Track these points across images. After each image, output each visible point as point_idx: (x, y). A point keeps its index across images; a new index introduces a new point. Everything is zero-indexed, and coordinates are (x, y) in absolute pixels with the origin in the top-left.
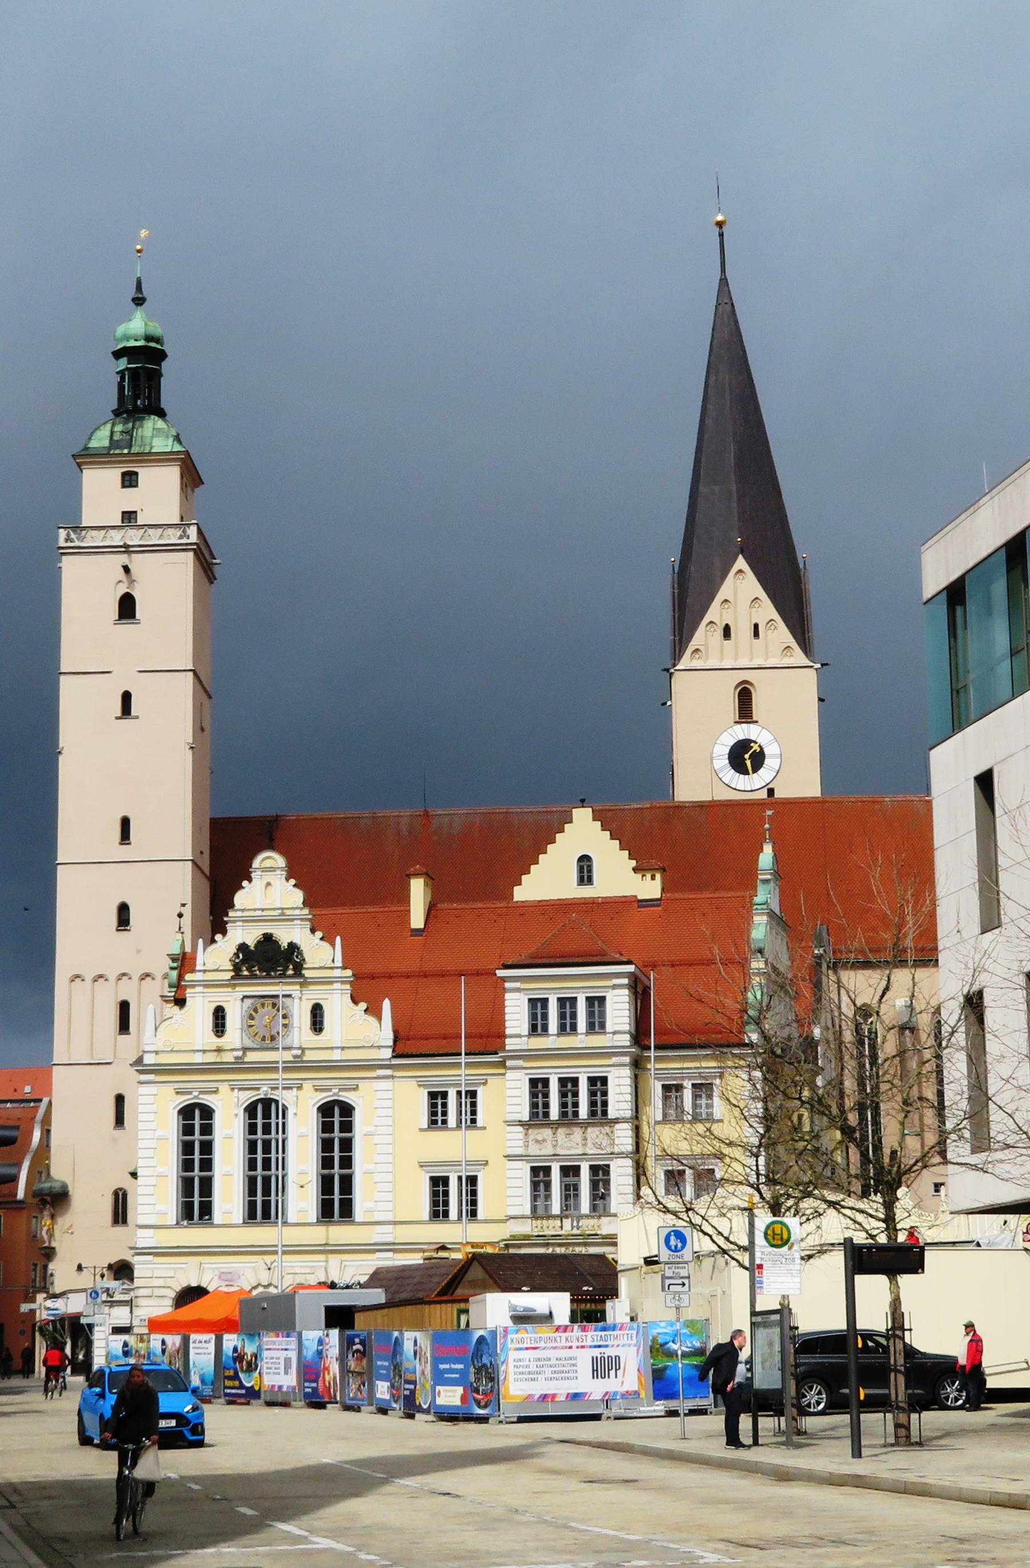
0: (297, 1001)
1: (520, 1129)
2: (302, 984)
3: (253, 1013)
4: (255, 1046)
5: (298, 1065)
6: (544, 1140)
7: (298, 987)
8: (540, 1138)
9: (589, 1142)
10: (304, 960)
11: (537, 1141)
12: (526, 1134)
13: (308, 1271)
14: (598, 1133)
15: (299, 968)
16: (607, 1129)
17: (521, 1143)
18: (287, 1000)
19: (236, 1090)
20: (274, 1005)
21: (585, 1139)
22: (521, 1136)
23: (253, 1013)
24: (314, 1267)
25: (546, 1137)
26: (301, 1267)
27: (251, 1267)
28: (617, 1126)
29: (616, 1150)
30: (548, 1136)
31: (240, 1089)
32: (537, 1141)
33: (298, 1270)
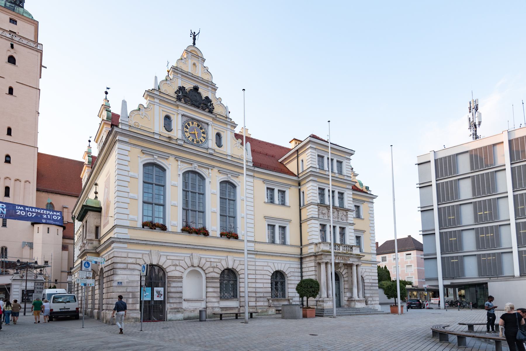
0: (210, 127)
2: (214, 119)
3: (188, 126)
4: (188, 143)
5: (211, 156)
7: (211, 120)
10: (214, 109)
13: (217, 261)
15: (211, 111)
18: (205, 126)
19: (179, 162)
20: (198, 126)
23: (188, 126)
24: (219, 259)
26: (214, 258)
27: (188, 257)
31: (181, 161)
33: (212, 260)
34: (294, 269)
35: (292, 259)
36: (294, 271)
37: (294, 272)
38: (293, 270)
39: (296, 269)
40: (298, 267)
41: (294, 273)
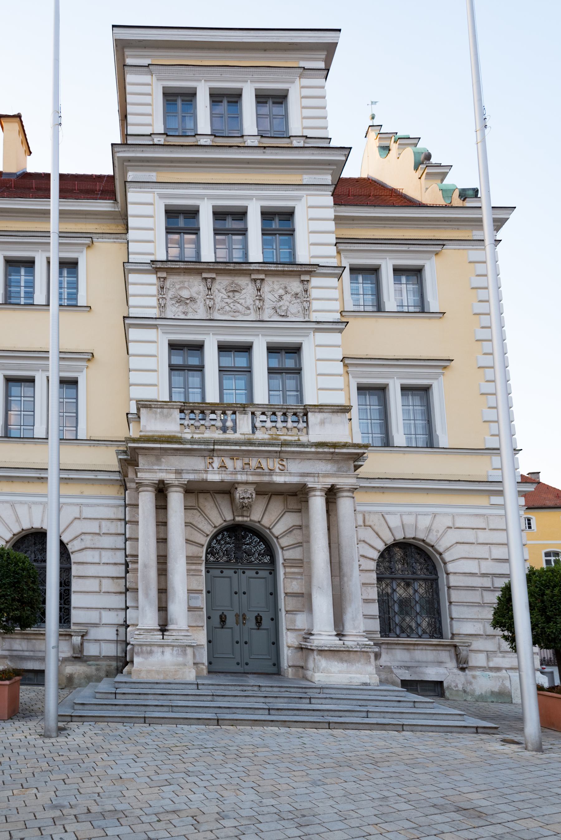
1: (152, 278)
6: (192, 299)
8: (185, 294)
9: (268, 304)
11: (180, 301)
12: (162, 288)
14: (281, 292)
16: (295, 286)
17: (153, 301)
21: (261, 299)
22: (154, 290)
25: (195, 295)
28: (315, 281)
29: (314, 317)
30: (198, 293)
32: (180, 301)
34: (96, 523)
35: (89, 490)
36: (98, 531)
37: (99, 534)
38: (93, 527)
39: (104, 523)
40: (113, 516)
41: (97, 537)
